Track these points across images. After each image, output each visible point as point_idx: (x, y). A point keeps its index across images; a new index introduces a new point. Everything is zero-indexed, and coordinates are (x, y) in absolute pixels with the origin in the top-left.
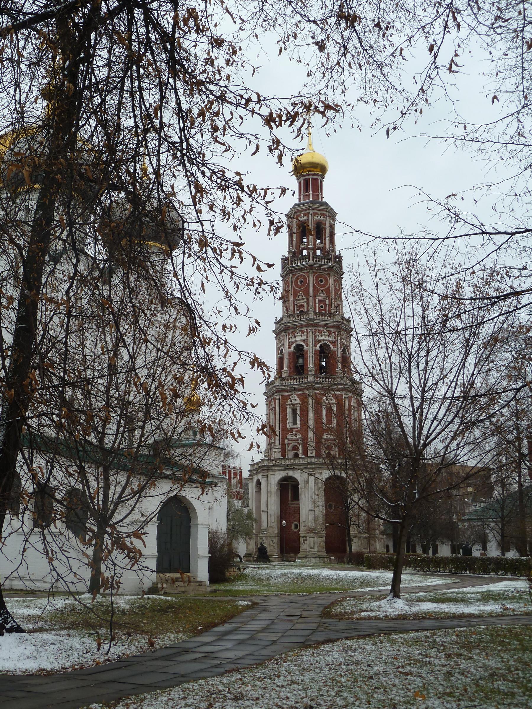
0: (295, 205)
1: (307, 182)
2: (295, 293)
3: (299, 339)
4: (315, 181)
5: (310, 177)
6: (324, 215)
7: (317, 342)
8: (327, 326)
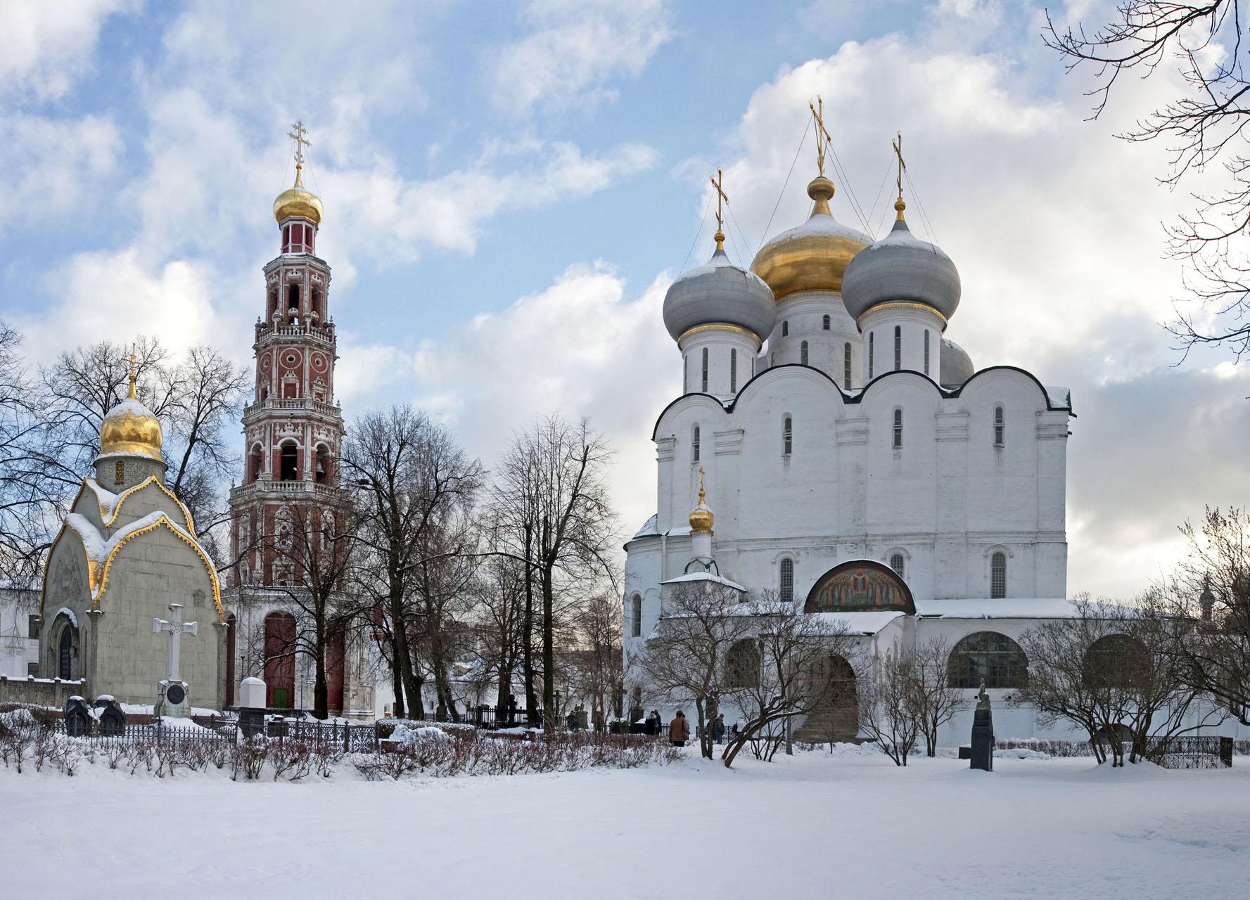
1: (297, 228)
3: (288, 435)
4: (308, 230)
5: (304, 224)
7: (313, 440)
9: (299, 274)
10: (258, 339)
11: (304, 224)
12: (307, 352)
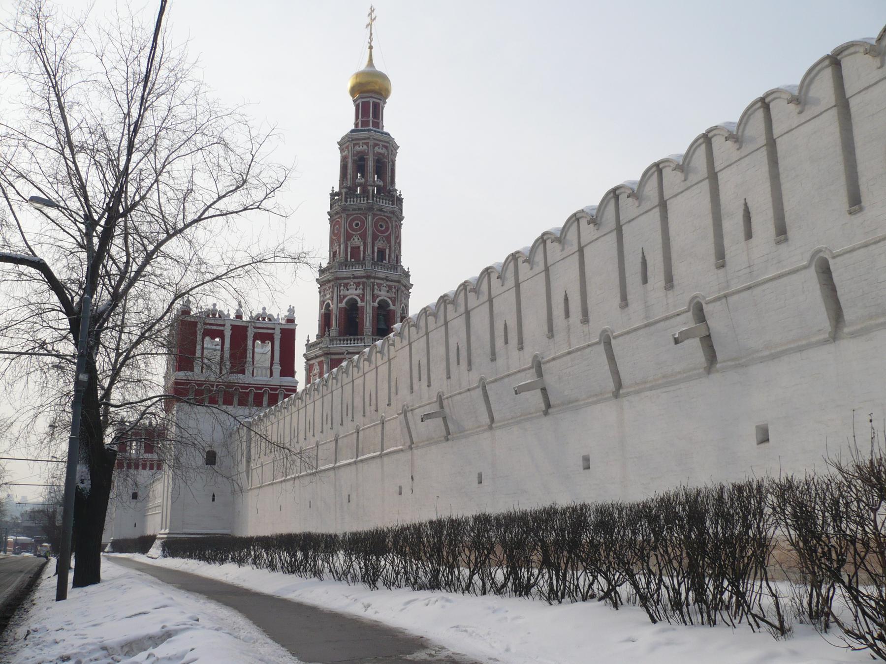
0: (352, 131)
2: (349, 237)
3: (353, 293)
6: (386, 147)
7: (374, 297)
8: (386, 279)
9: (365, 147)
10: (331, 208)
11: (371, 101)
12: (370, 218)
